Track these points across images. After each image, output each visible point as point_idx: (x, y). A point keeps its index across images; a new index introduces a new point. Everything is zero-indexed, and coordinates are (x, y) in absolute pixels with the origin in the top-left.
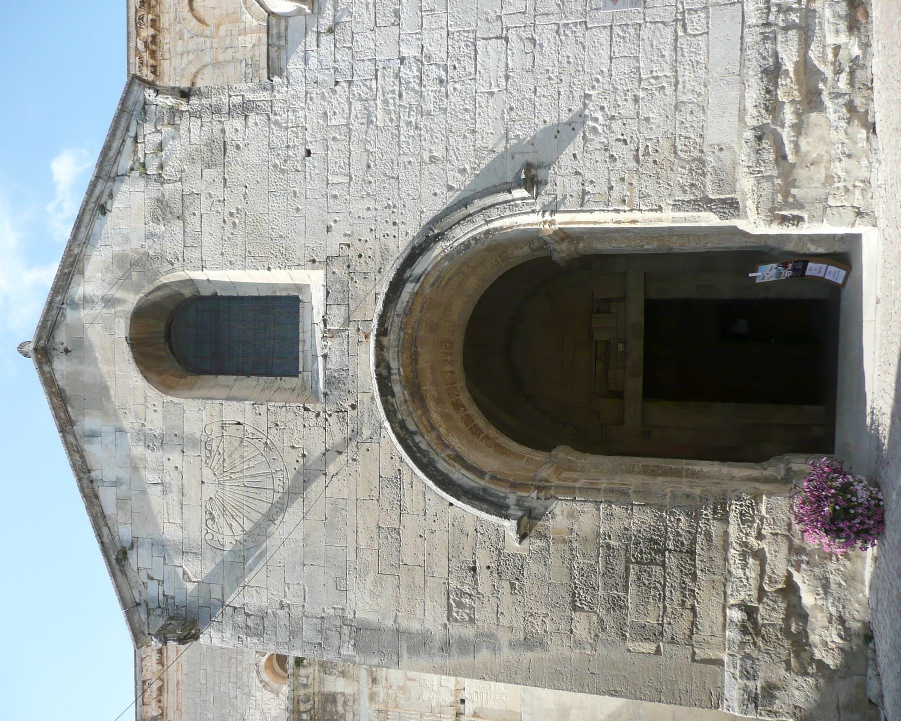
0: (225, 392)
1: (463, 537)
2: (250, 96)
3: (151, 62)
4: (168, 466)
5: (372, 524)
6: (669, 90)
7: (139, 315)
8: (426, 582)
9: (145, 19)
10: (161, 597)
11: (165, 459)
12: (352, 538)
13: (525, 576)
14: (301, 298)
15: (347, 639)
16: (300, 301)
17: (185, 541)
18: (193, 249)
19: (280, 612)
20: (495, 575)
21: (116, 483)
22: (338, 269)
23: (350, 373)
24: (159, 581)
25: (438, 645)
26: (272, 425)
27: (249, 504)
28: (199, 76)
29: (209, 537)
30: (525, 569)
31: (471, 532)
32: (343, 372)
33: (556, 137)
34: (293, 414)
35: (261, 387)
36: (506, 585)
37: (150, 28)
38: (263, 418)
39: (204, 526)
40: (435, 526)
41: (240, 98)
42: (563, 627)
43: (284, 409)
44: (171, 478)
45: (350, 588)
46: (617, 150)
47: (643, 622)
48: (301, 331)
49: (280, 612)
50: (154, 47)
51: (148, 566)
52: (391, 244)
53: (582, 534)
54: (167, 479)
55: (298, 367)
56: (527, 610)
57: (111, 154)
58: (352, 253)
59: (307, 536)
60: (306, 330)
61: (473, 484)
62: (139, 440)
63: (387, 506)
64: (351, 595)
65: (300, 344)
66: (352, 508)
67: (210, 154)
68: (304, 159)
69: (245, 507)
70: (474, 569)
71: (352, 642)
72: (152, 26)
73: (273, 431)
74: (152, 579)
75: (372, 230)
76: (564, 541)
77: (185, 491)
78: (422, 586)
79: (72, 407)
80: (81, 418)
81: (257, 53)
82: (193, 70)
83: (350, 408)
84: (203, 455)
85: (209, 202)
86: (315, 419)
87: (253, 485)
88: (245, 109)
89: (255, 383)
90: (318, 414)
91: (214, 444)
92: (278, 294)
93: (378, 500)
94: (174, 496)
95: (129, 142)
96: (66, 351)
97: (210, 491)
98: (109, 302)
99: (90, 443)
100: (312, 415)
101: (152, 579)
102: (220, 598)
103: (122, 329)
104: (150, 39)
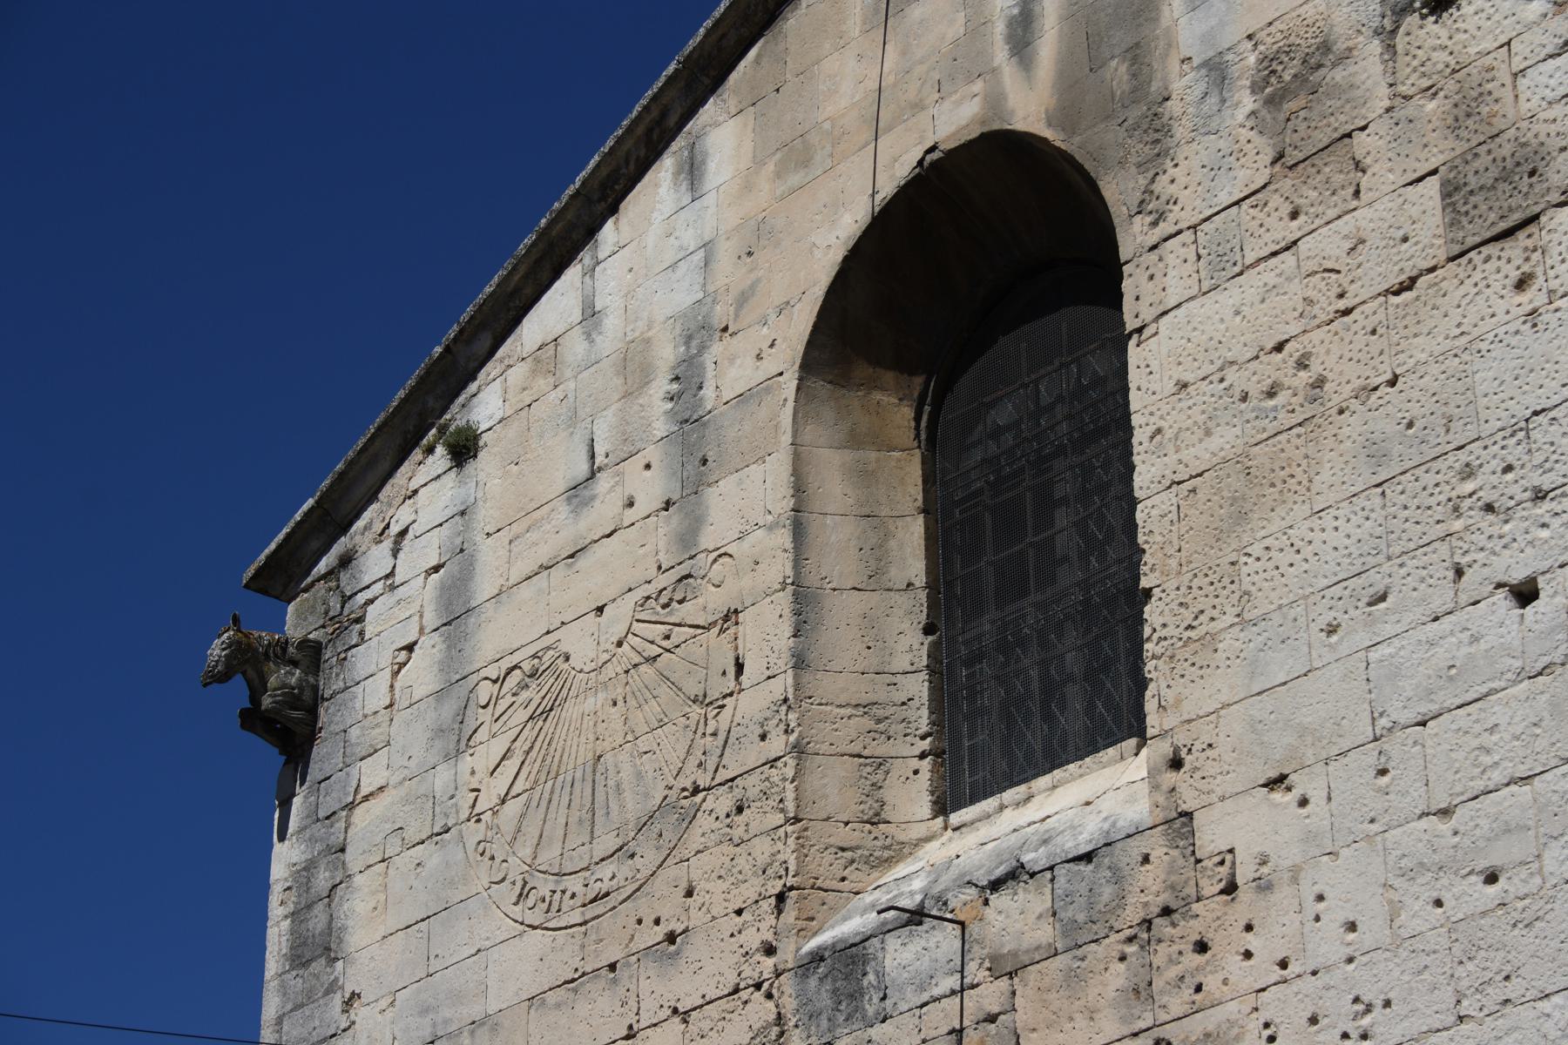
10: (361, 598)
24: (391, 574)
35: (881, 695)
43: (779, 819)
48: (1058, 774)
55: (957, 807)
58: (1208, 915)
65: (1022, 788)
68: (1499, 586)
69: (550, 783)
75: (1283, 965)
87: (600, 797)
90: (770, 950)
94: (563, 527)
97: (582, 644)
102: (364, 791)
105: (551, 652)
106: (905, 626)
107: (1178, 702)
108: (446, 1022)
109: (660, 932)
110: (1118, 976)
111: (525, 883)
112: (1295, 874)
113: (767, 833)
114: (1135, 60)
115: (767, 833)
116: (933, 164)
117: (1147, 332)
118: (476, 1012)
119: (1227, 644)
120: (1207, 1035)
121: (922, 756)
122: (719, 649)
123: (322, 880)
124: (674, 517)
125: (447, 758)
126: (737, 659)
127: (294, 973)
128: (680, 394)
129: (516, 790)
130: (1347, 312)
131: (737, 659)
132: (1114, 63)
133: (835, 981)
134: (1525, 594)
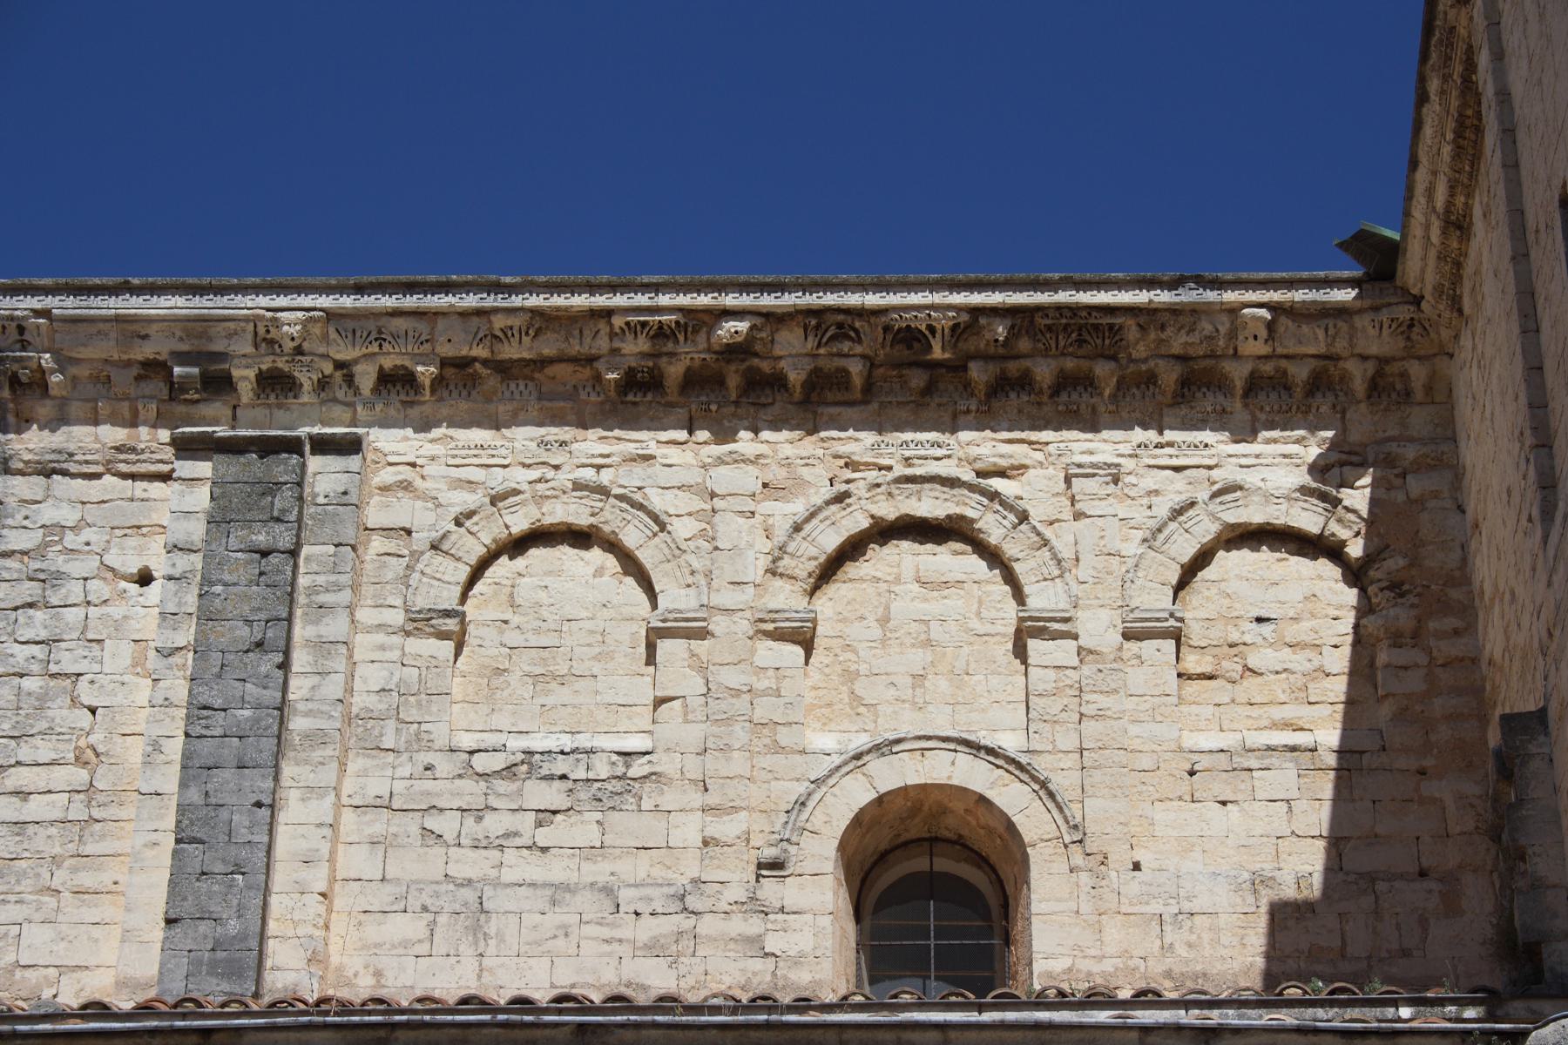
3: (674, 371)
9: (846, 346)
28: (611, 562)
37: (808, 365)
50: (733, 381)
72: (816, 371)
81: (669, 799)
82: (631, 537)
104: (765, 366)
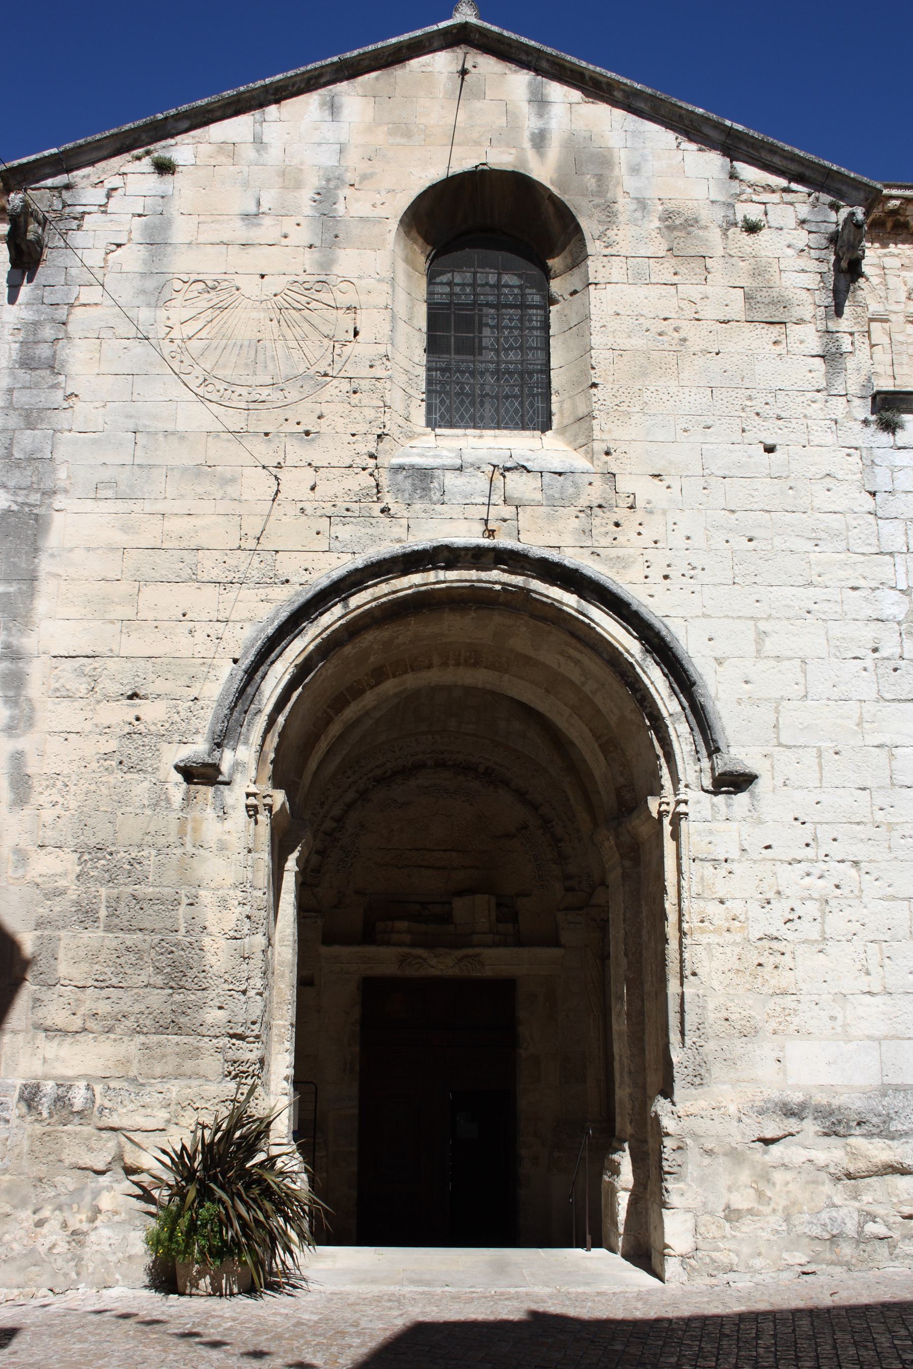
0: (402, 310)
1: (185, 680)
2: (850, 363)
4: (288, 225)
5: (203, 540)
6: (863, 983)
7: (519, 184)
8: (112, 622)
10: (81, 209)
11: (300, 219)
12: (179, 506)
13: (128, 776)
14: (549, 433)
15: (20, 500)
16: (543, 432)
17: (169, 249)
18: (624, 271)
19: (60, 394)
20: (127, 729)
21: (258, 141)
22: (595, 493)
23: (438, 507)
24: (105, 205)
25: (14, 641)
26: (355, 385)
27: (229, 349)
29: (178, 285)
30: (136, 776)
31: (194, 692)
32: (438, 494)
33: (796, 819)
34: (372, 417)
35: (410, 369)
36: (113, 745)
38: (366, 372)
39: (194, 277)
40: (200, 636)
41: (850, 349)
42: (50, 836)
44: (268, 229)
45: (102, 503)
46: (780, 909)
47: (61, 955)
49: (60, 394)
51: (130, 190)
52: (636, 572)
53: (195, 862)
54: (267, 221)
55: (440, 427)
56: (74, 777)
57: (765, 155)
58: (621, 514)
59: (182, 437)
60: (499, 439)
61: (267, 694)
62: (328, 180)
63: (232, 562)
64: (90, 505)
66: (225, 506)
67: (767, 300)
70: (134, 696)
71: (15, 507)
73: (346, 386)
74: (108, 196)
75: (656, 542)
76: (182, 834)
77: (251, 250)
78: (107, 617)
79: (377, 78)
80: (360, 91)
83: (382, 505)
84: (307, 278)
85: (696, 297)
86: (365, 450)
88: (832, 357)
89: (417, 360)
91: (324, 296)
92: (554, 398)
93: (239, 548)
94: (240, 231)
95: (783, 182)
96: (464, 72)
97: (250, 286)
98: (540, 140)
99: (323, 104)
100: (371, 447)
101: (108, 196)
102: (82, 301)
103: (501, 159)
105: (226, 283)
106: (418, 345)
107: (610, 431)
108: (145, 426)
109: (301, 429)
110: (574, 523)
111: (205, 380)
112: (664, 512)
113: (374, 407)
114: (599, 180)
115: (374, 407)
116: (482, 170)
117: (598, 286)
118: (170, 427)
119: (636, 417)
120: (618, 557)
121: (422, 400)
122: (346, 322)
123: (48, 332)
124: (315, 254)
125: (149, 305)
126: (355, 328)
127: (23, 371)
128: (321, 202)
129: (202, 334)
130: (698, 320)
131: (355, 328)
132: (589, 176)
133: (414, 480)
134: (770, 449)
